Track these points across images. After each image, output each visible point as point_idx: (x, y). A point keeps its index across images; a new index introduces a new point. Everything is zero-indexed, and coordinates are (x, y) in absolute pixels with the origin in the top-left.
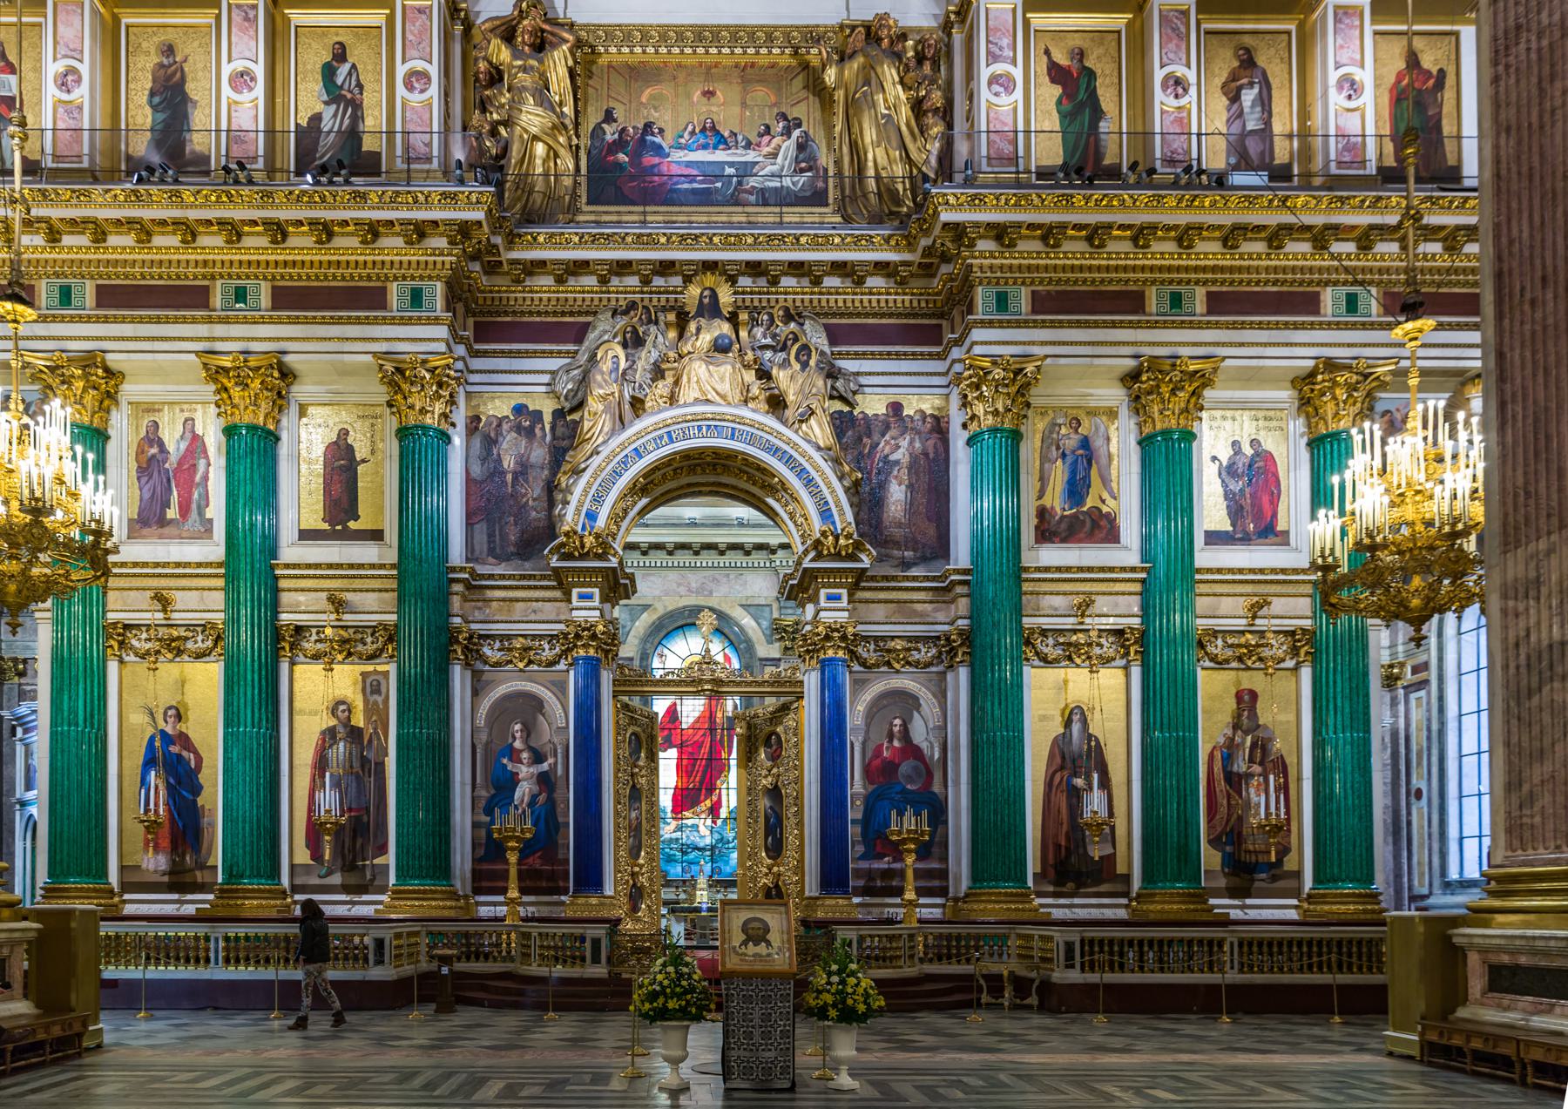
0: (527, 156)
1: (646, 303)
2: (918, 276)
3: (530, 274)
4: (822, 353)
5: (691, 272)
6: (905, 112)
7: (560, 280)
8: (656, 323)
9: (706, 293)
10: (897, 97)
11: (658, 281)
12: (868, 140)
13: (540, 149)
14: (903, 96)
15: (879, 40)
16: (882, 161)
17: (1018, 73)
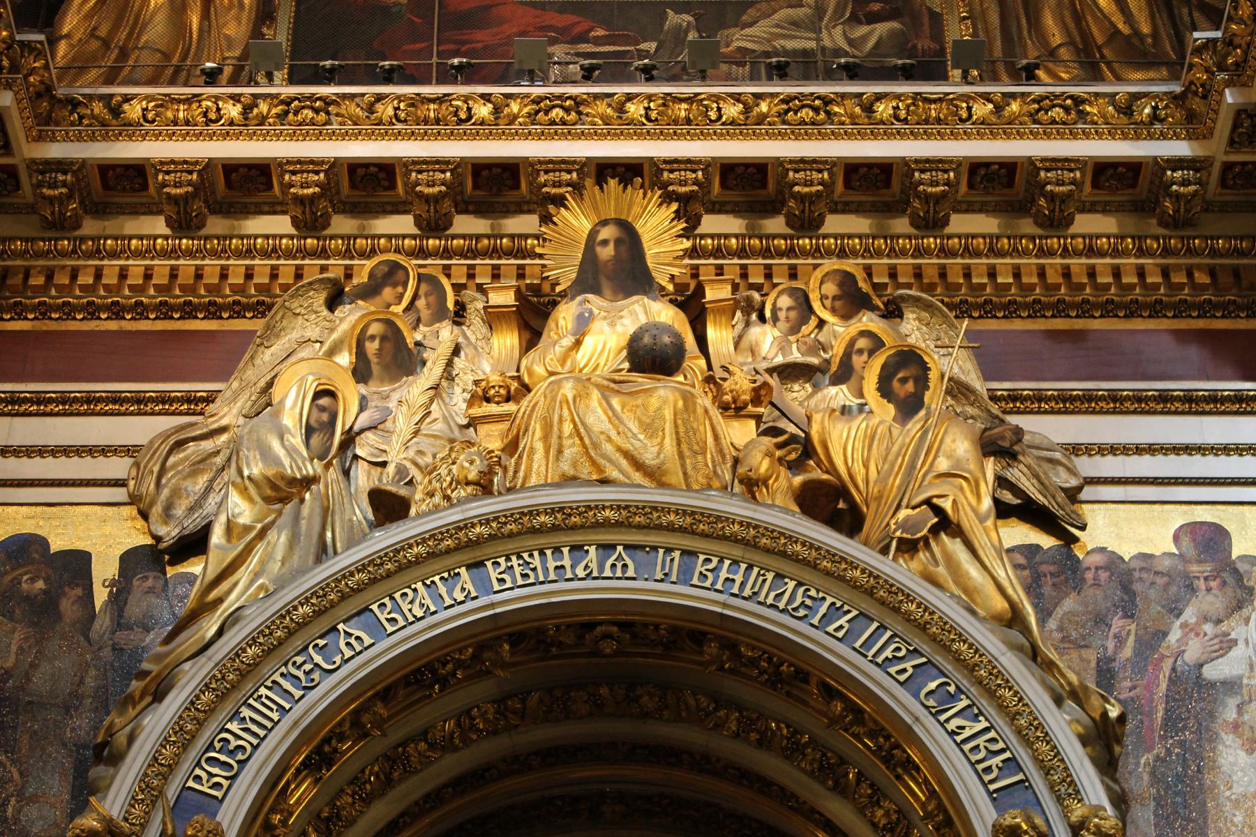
2: (1225, 208)
3: (101, 210)
7: (184, 224)
9: (607, 233)
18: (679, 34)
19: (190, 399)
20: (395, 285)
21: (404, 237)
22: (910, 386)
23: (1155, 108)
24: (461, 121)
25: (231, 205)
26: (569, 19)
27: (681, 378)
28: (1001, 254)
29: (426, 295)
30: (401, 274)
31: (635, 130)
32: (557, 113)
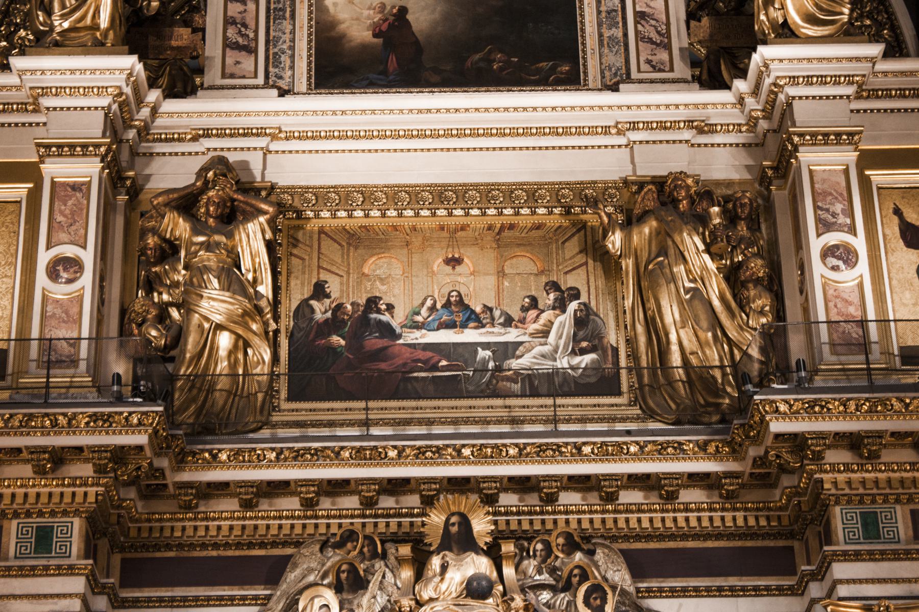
0: (207, 347)
1: (369, 530)
4: (623, 593)
5: (431, 493)
6: (715, 289)
7: (247, 505)
8: (384, 556)
9: (454, 519)
10: (705, 268)
11: (387, 502)
12: (668, 319)
13: (225, 341)
14: (712, 266)
15: (675, 202)
16: (690, 344)
17: (859, 243)
18: (485, 362)
19: (256, 598)
20: (352, 542)
21: (355, 509)
22: (598, 602)
23: (717, 447)
24: (382, 459)
25: (270, 493)
26: (429, 354)
27: (490, 600)
28: (643, 511)
29: (368, 546)
30: (355, 536)
31: (467, 461)
32: (429, 454)
